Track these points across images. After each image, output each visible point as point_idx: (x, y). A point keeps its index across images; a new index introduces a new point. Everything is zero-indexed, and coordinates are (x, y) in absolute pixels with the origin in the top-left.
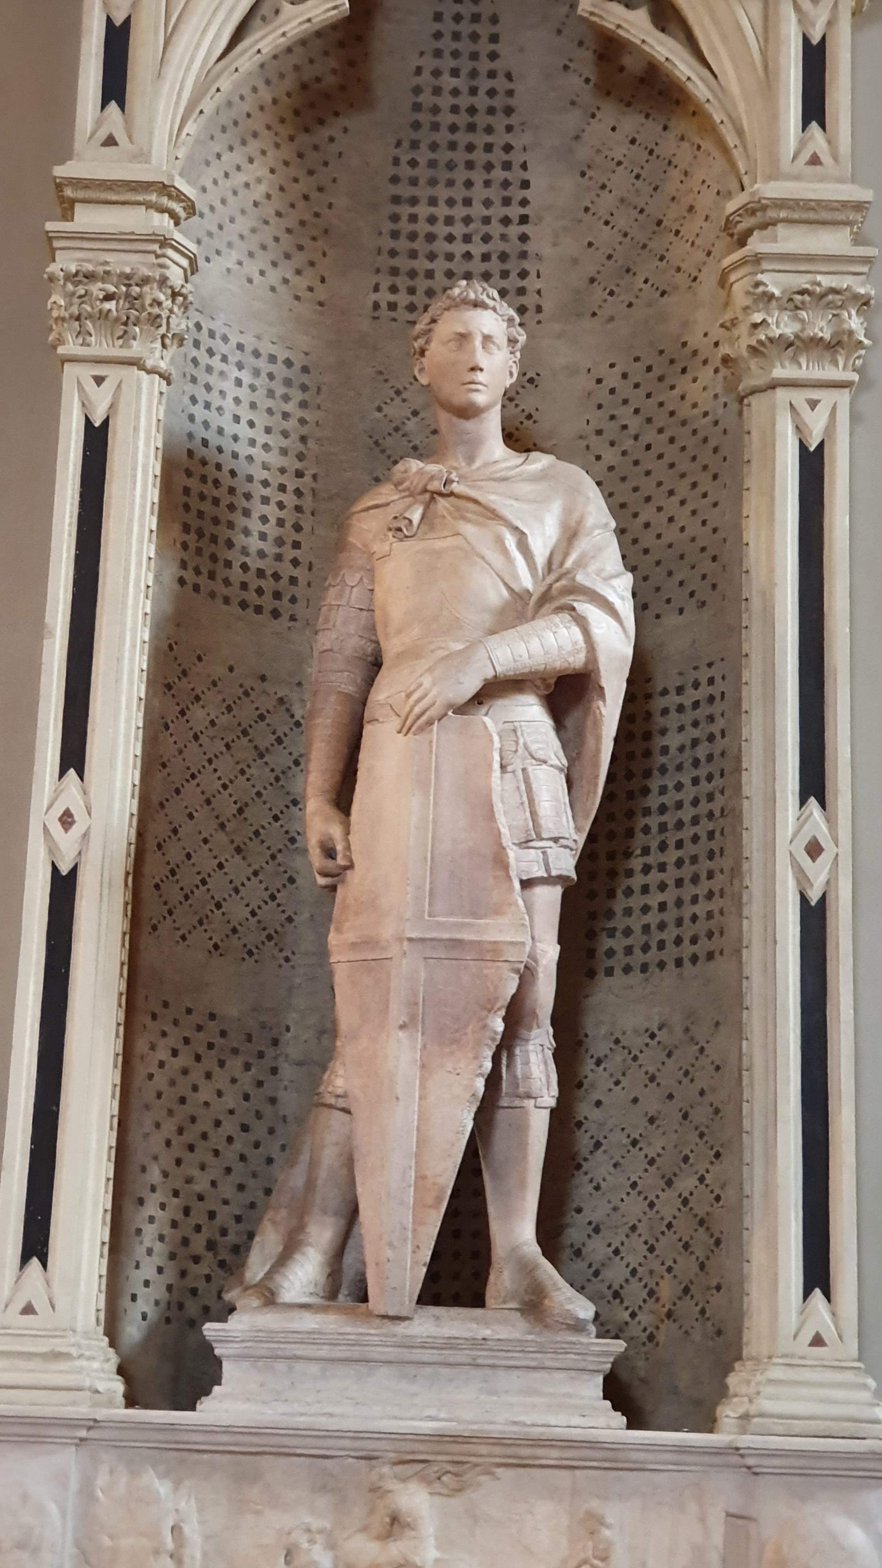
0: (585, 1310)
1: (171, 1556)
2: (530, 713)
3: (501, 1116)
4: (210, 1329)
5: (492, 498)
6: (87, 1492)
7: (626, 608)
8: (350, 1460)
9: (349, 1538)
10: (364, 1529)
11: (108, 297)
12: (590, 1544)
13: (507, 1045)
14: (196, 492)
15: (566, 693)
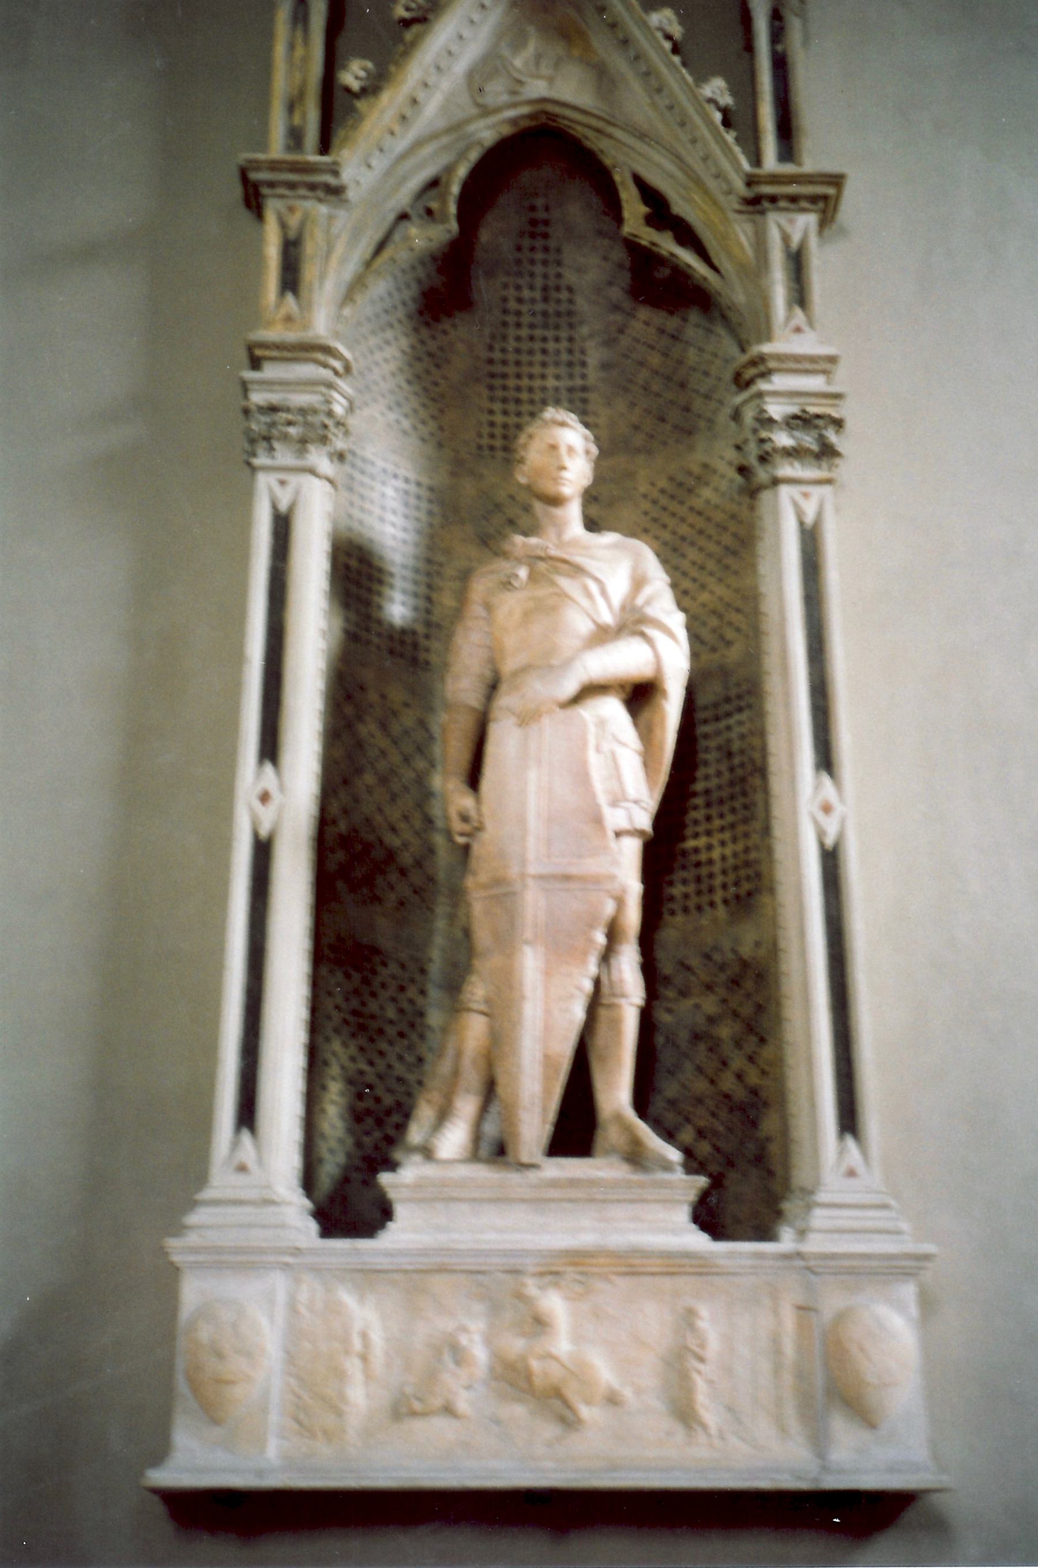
0: (674, 1155)
2: (612, 709)
3: (603, 1013)
4: (385, 1178)
5: (579, 560)
7: (682, 634)
11: (290, 423)
13: (607, 956)
14: (355, 572)
15: (640, 695)
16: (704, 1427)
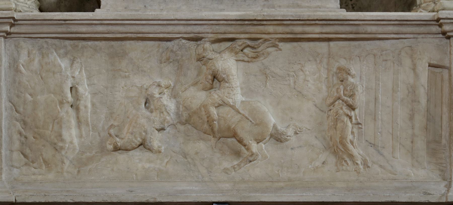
1: (72, 106)
6: (14, 66)
8: (184, 41)
9: (186, 89)
10: (195, 84)
12: (341, 87)
16: (351, 156)
